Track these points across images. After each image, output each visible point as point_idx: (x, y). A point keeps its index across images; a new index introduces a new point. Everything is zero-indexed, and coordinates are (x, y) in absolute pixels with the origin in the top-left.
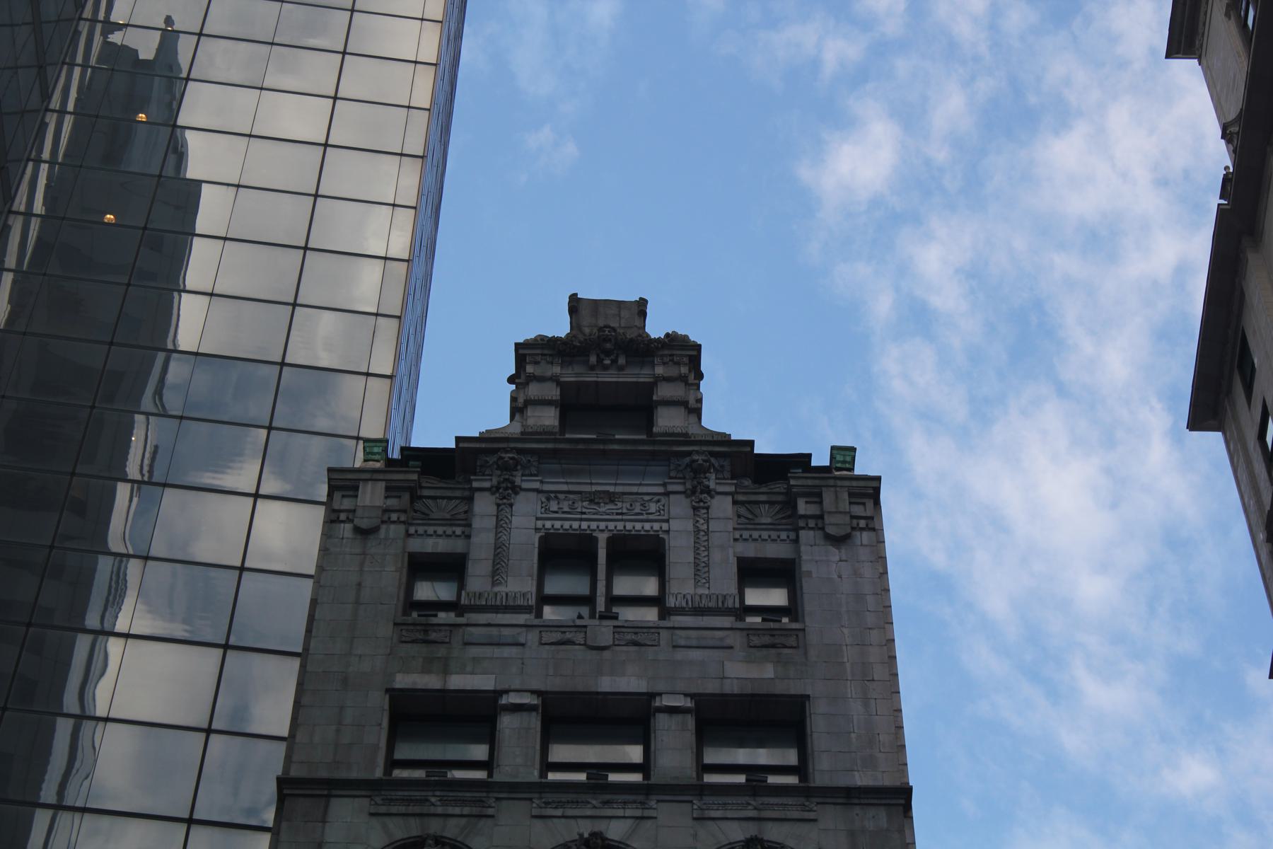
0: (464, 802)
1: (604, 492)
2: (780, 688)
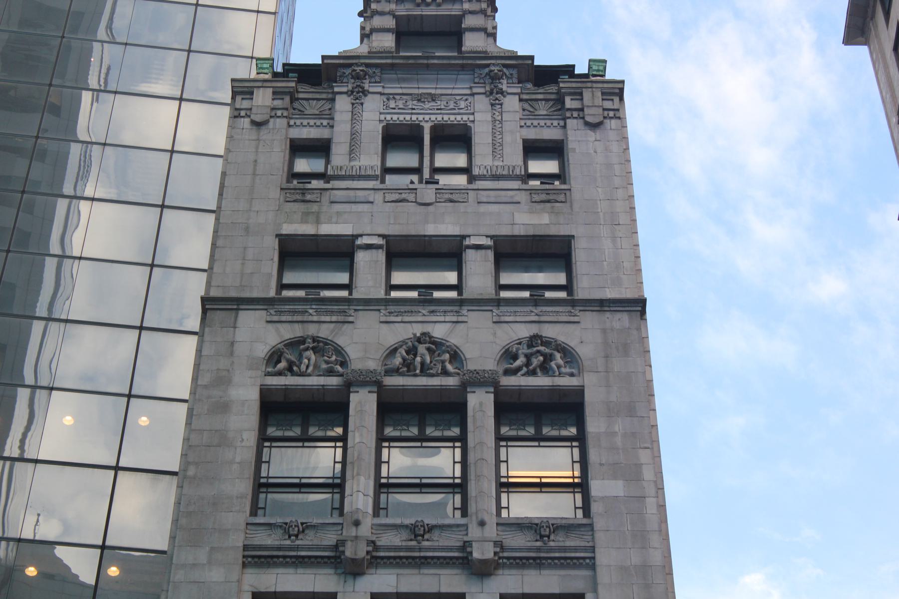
0: (332, 313)
1: (428, 94)
2: (553, 231)
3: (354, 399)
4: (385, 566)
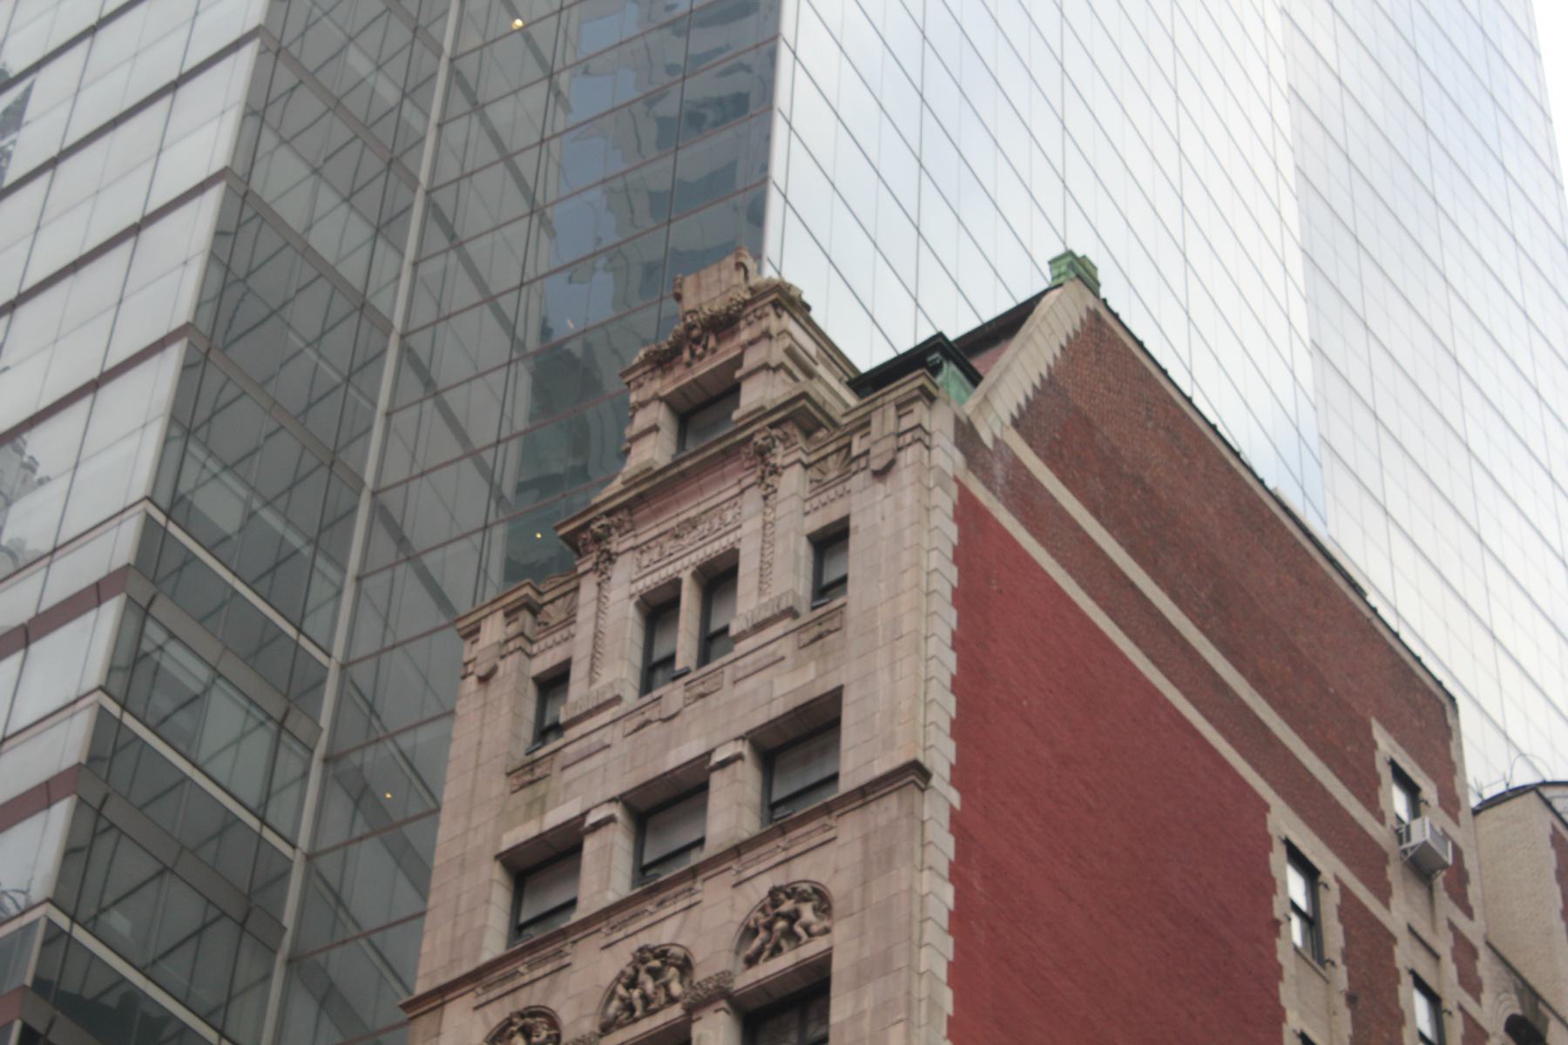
0: (545, 960)
3: (697, 1030)
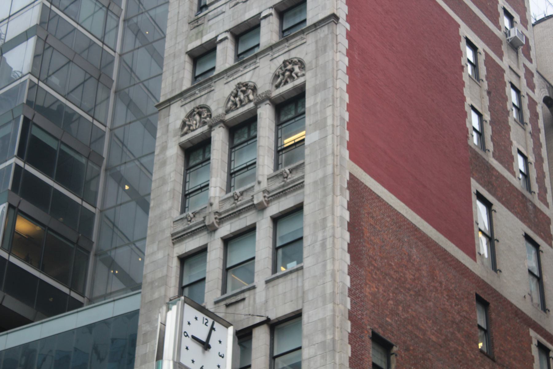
0: (205, 88)
3: (259, 111)
4: (226, 221)
